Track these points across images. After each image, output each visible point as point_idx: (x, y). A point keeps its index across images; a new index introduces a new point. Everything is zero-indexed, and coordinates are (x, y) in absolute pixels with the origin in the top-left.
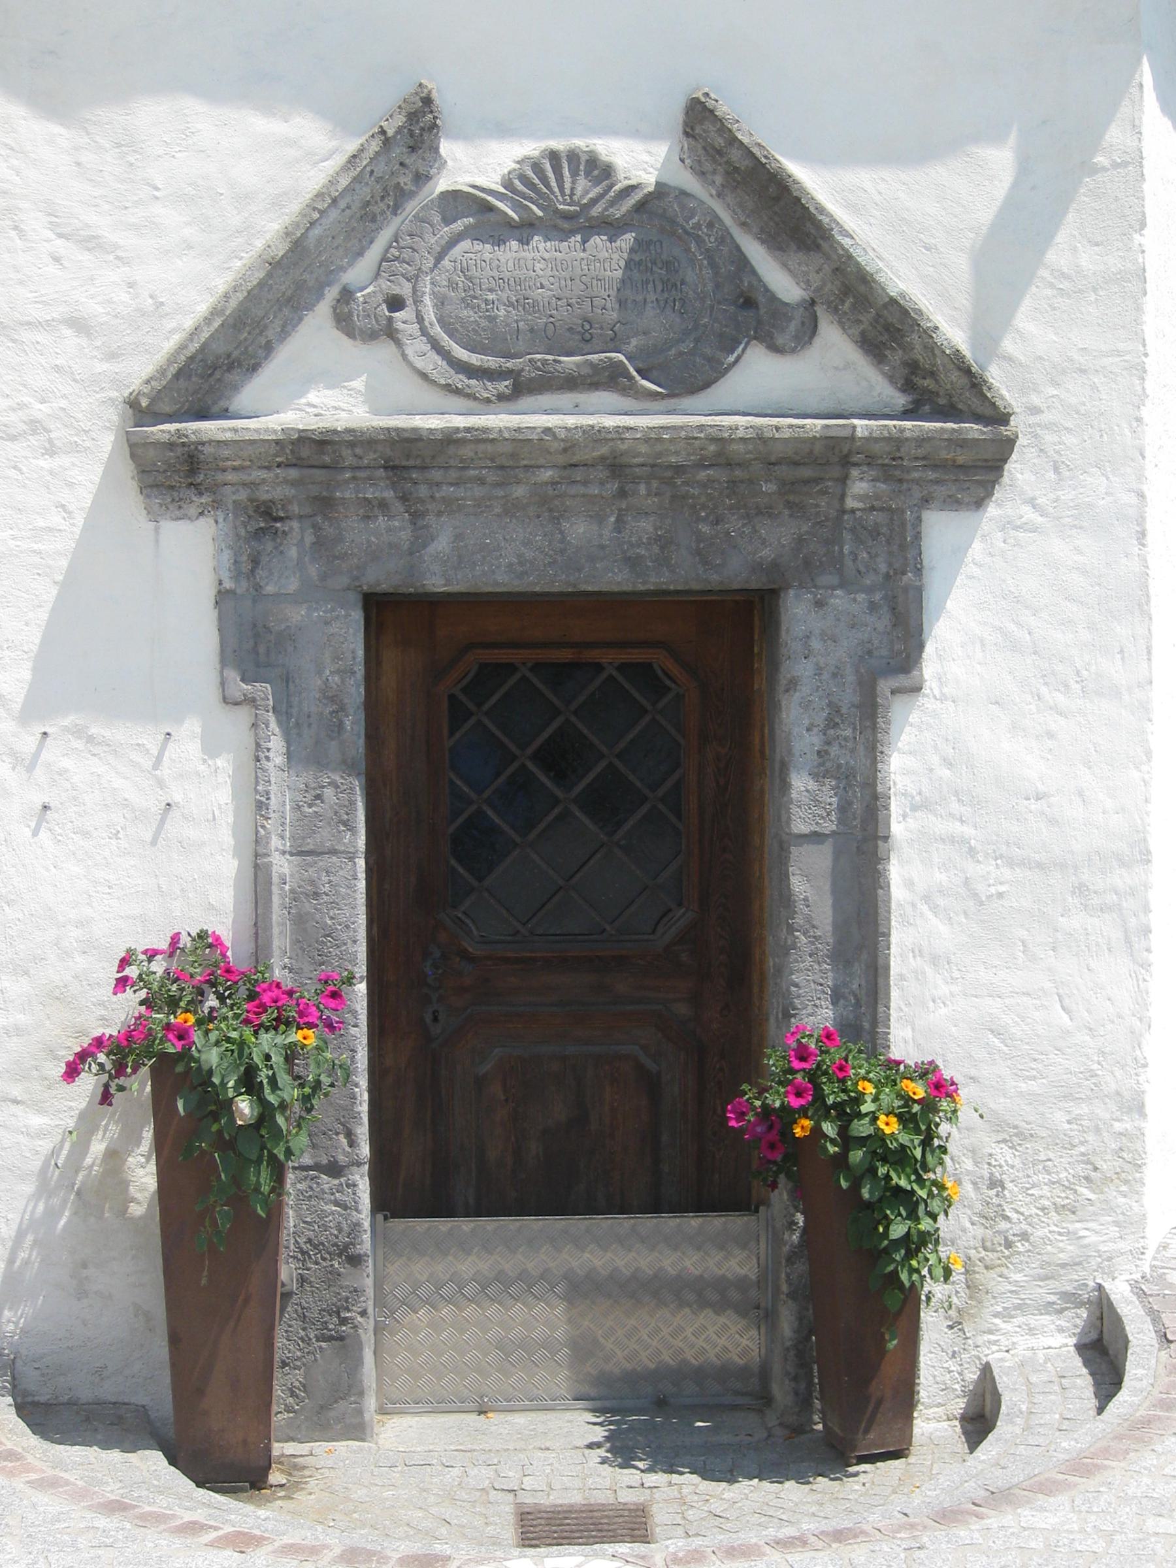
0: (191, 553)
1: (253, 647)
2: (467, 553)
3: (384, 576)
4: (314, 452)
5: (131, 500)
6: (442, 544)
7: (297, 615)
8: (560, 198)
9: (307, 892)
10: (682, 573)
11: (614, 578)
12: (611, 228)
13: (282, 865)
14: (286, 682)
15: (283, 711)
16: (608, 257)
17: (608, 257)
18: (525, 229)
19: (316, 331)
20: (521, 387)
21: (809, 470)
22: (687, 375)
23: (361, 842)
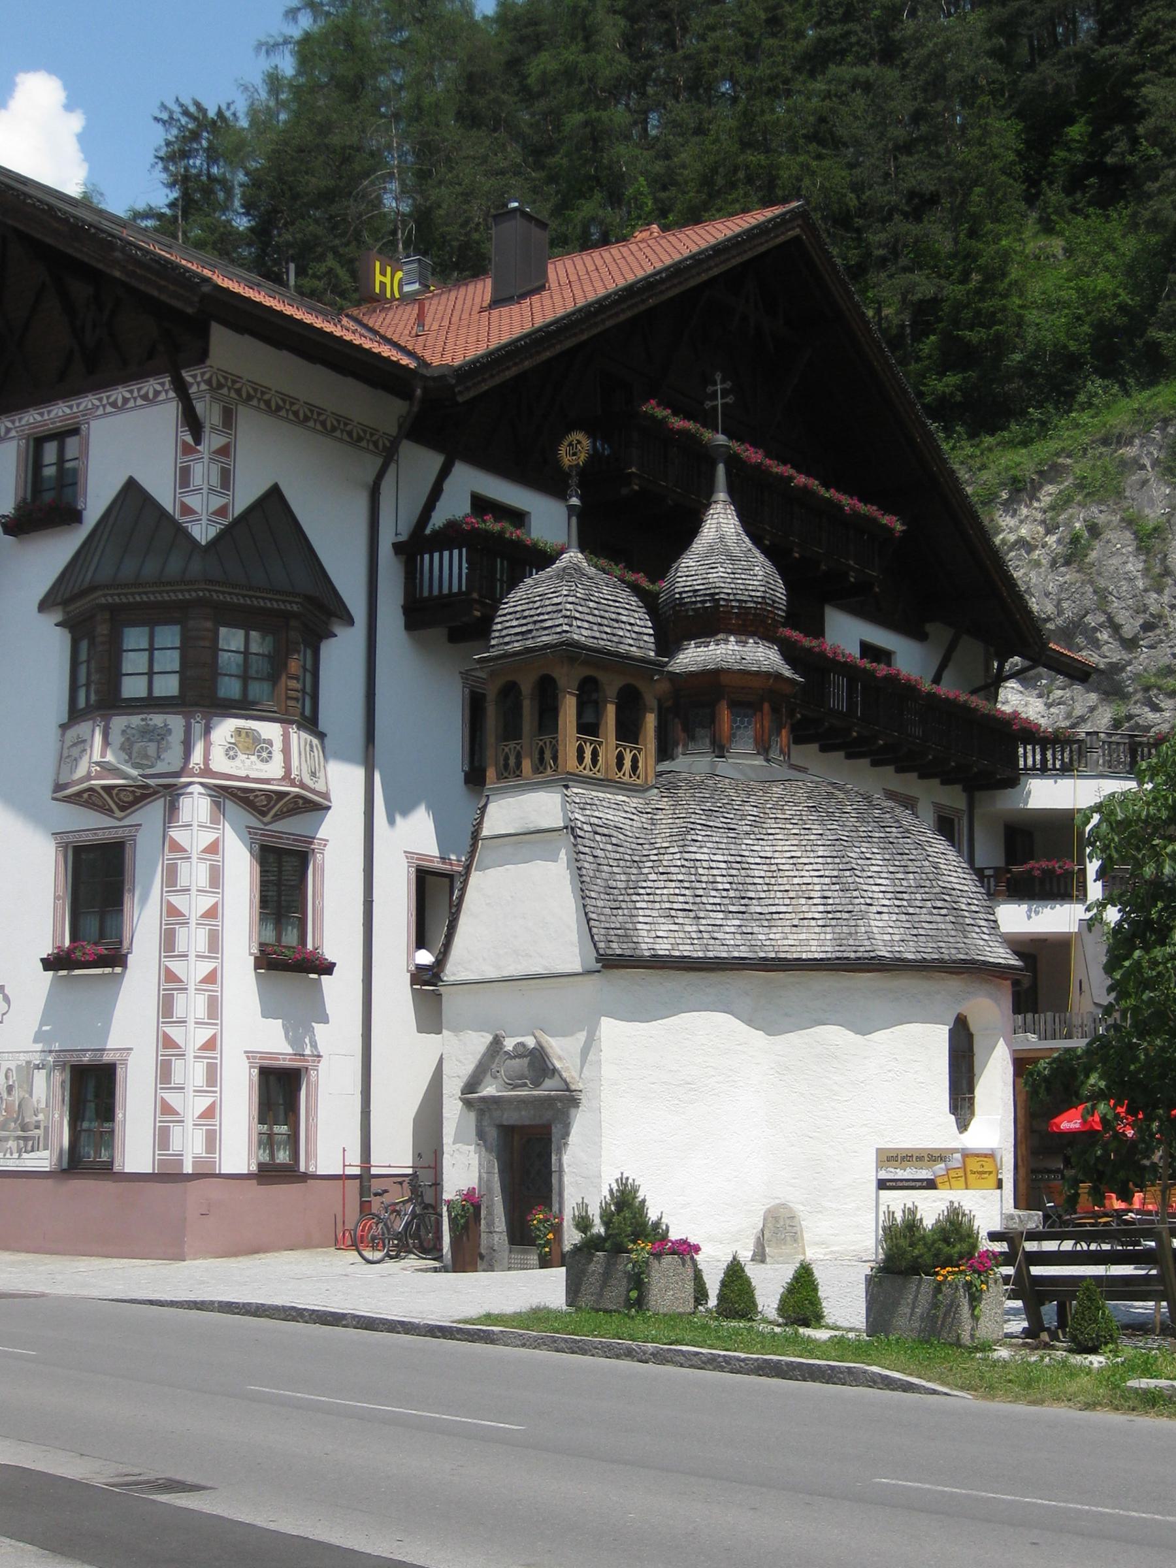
0: (472, 1116)
1: (481, 1134)
2: (511, 1117)
3: (497, 1122)
4: (483, 1099)
5: (465, 1110)
6: (505, 1116)
7: (487, 1129)
8: (521, 1052)
9: (488, 1180)
10: (537, 1122)
11: (527, 1123)
12: (525, 1056)
13: (485, 1176)
14: (485, 1141)
15: (485, 1146)
16: (526, 1061)
17: (526, 1061)
18: (515, 1057)
19: (488, 1078)
20: (515, 1087)
21: (549, 1101)
22: (537, 1084)
23: (496, 1171)
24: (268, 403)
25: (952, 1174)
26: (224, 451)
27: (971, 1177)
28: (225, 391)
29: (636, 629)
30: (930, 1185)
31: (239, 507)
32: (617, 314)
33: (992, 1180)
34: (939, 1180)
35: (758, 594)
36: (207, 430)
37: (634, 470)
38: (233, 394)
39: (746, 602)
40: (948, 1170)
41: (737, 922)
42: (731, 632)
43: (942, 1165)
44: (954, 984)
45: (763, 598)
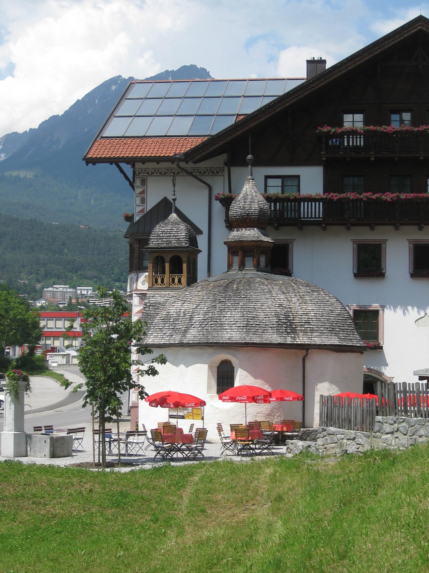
24: (161, 173)
25: (189, 414)
26: (142, 192)
27: (195, 415)
28: (142, 174)
29: (178, 237)
30: (183, 417)
31: (148, 209)
32: (284, 104)
33: (200, 417)
34: (185, 416)
35: (239, 213)
36: (135, 188)
37: (323, 153)
38: (145, 174)
39: (236, 216)
40: (188, 413)
41: (170, 332)
42: (236, 227)
43: (186, 411)
44: (210, 350)
45: (240, 214)
